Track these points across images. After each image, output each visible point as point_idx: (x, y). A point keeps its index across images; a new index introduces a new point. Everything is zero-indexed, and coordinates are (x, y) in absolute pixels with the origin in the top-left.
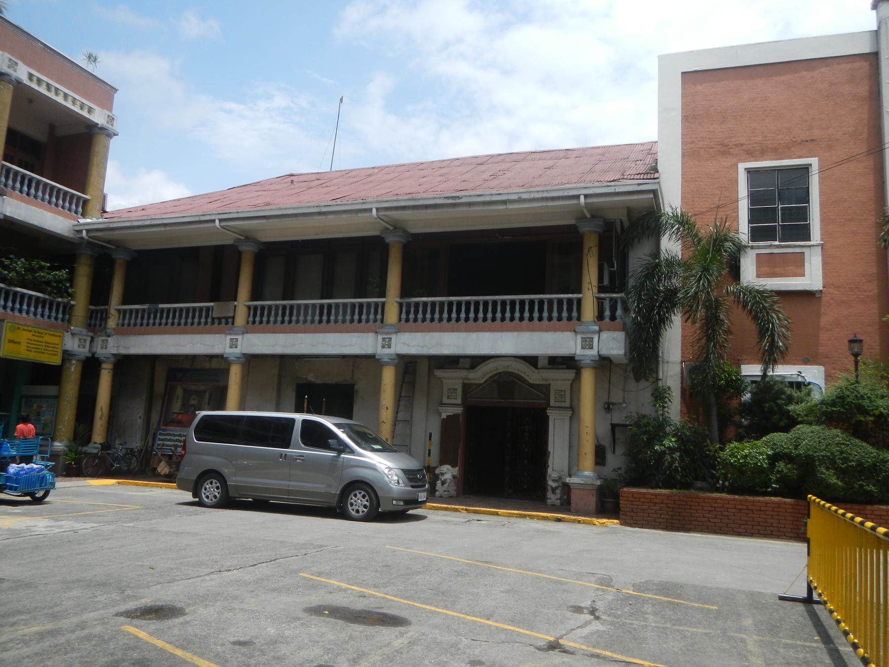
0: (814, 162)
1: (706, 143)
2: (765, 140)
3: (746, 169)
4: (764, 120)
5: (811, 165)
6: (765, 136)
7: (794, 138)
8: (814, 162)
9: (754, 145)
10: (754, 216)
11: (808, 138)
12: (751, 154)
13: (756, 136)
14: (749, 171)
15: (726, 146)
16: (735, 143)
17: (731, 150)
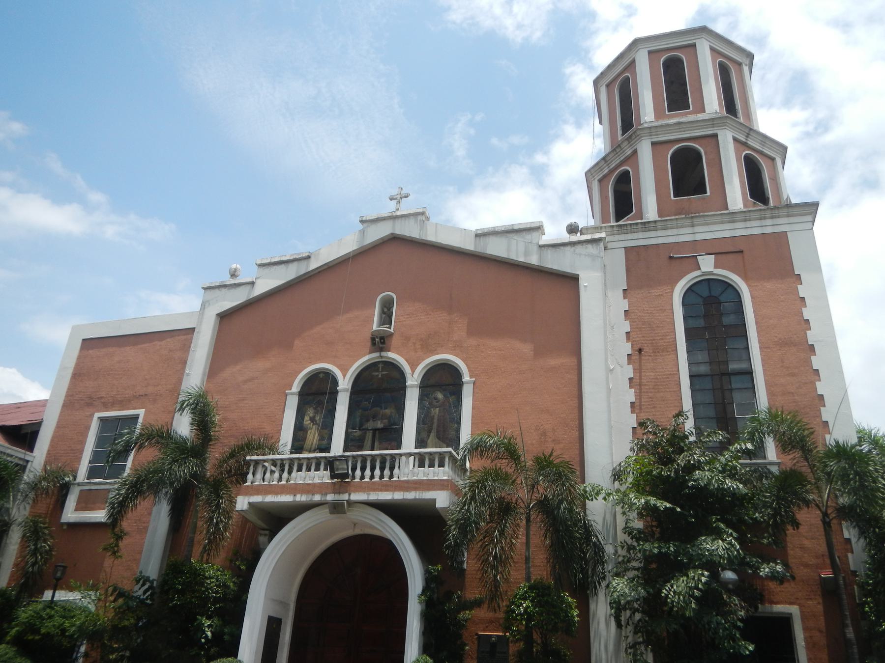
0: (141, 412)
1: (80, 396)
2: (116, 395)
3: (99, 418)
4: (122, 378)
5: (139, 415)
6: (118, 391)
7: (135, 393)
8: (141, 412)
9: (110, 398)
10: (96, 456)
11: (144, 394)
12: (106, 407)
13: (112, 391)
14: (102, 420)
15: (92, 399)
16: (98, 397)
17: (94, 402)
